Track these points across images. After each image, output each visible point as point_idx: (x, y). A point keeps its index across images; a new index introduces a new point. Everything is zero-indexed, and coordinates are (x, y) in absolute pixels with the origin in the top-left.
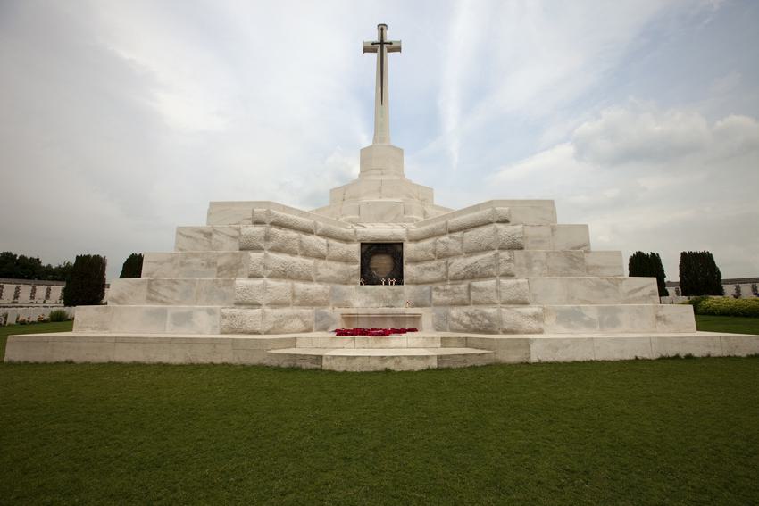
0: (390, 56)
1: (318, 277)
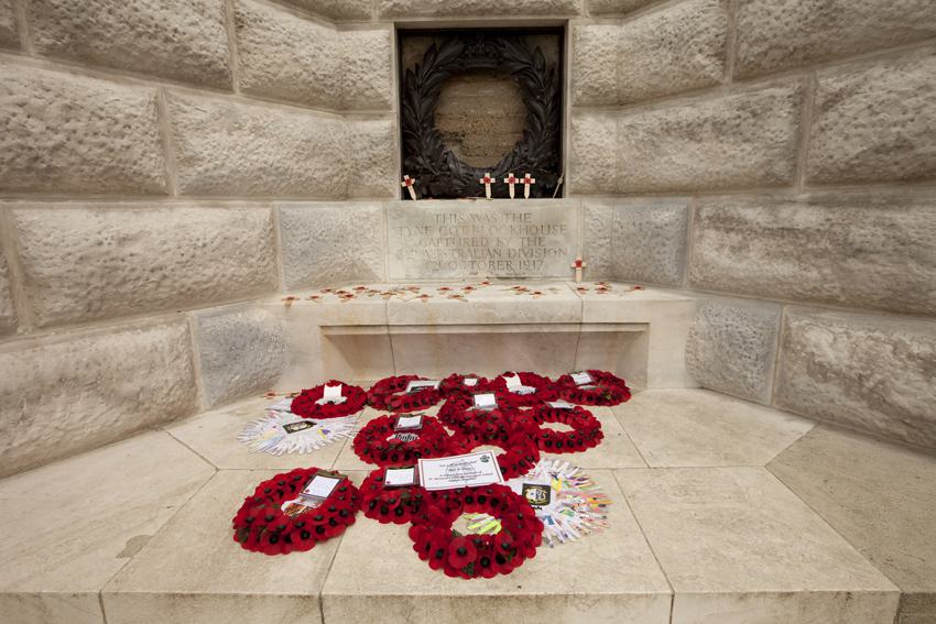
1: (192, 173)
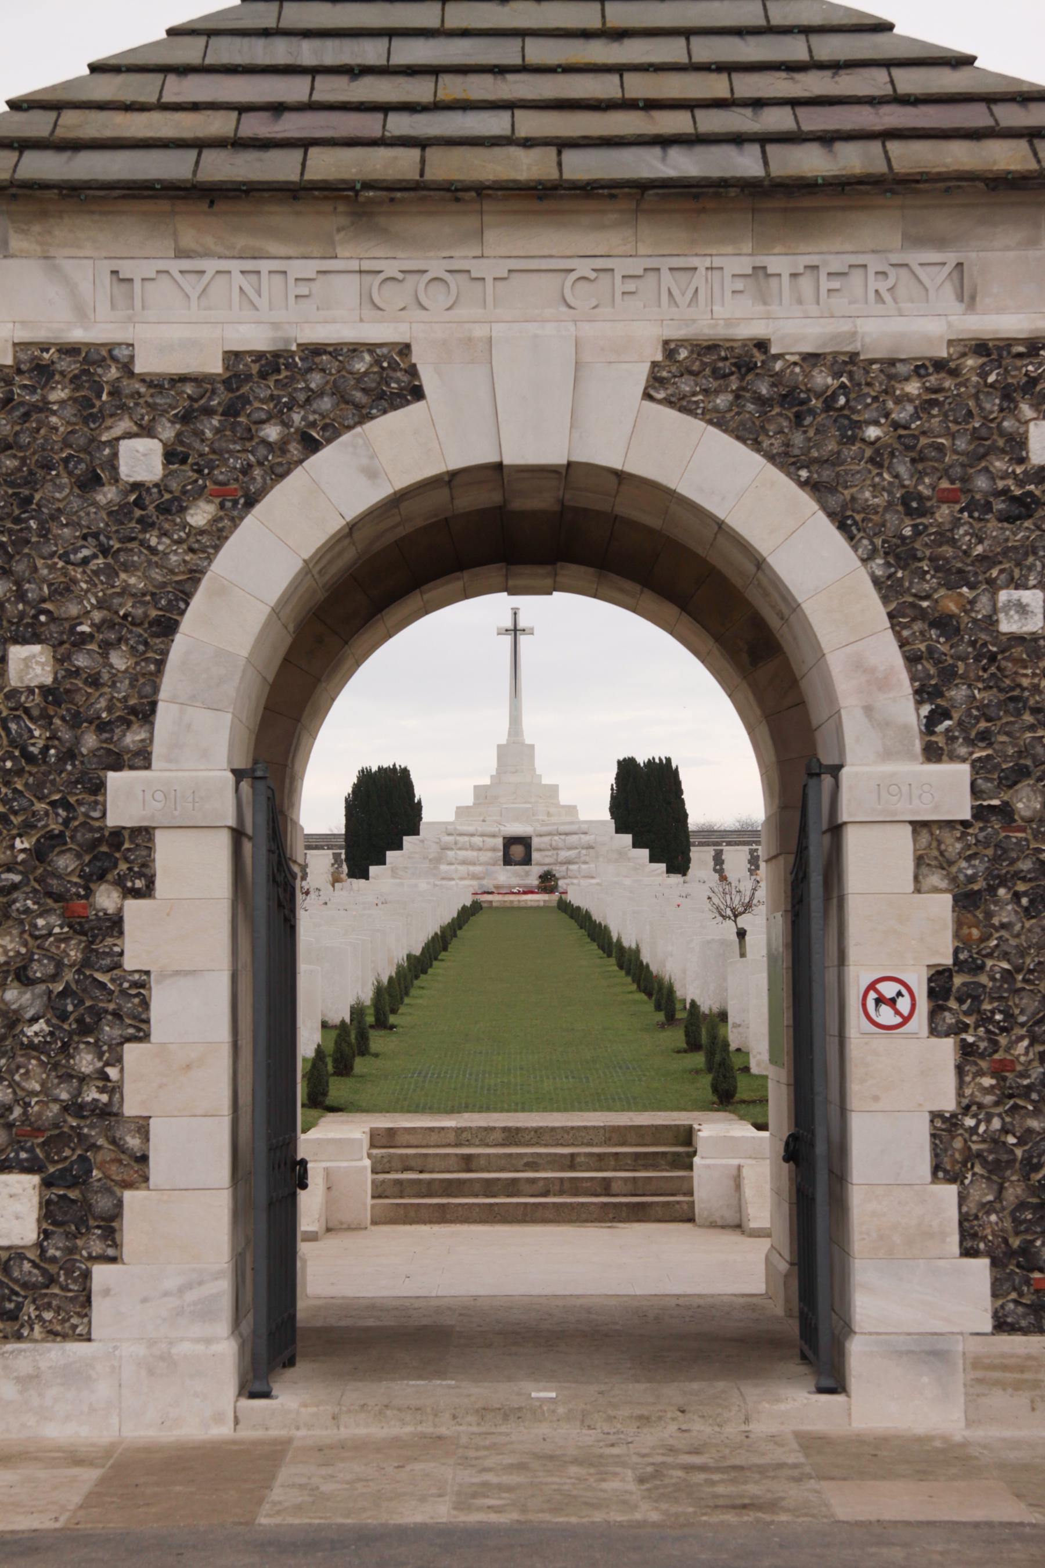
0: (523, 639)
